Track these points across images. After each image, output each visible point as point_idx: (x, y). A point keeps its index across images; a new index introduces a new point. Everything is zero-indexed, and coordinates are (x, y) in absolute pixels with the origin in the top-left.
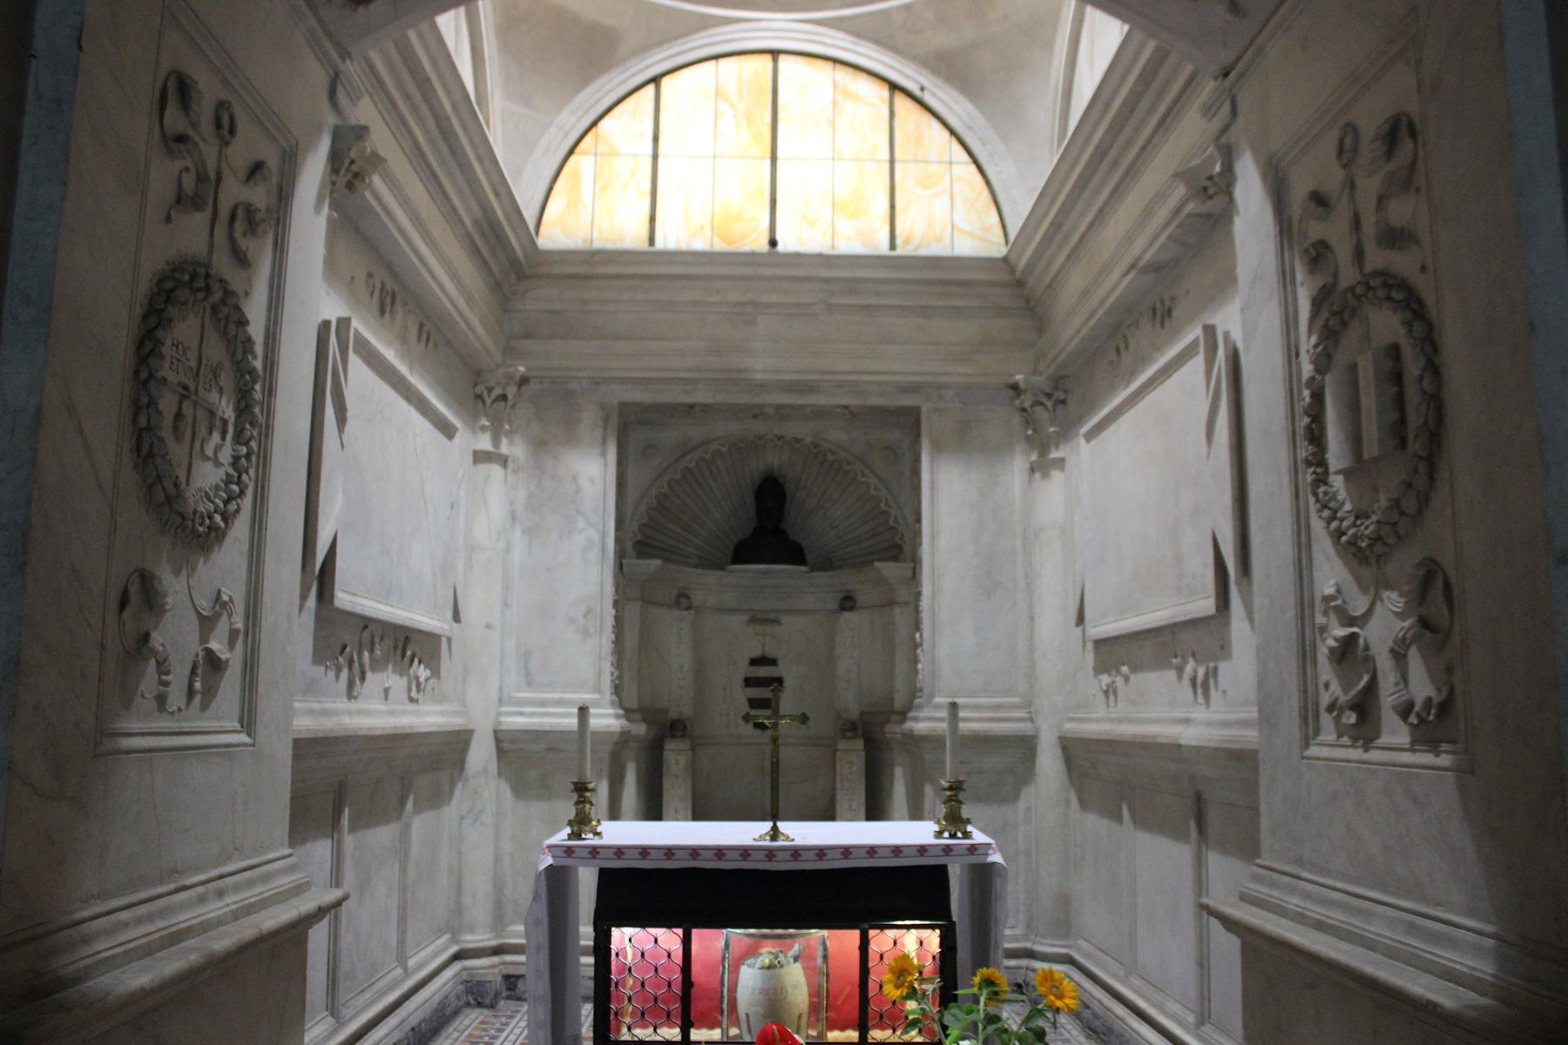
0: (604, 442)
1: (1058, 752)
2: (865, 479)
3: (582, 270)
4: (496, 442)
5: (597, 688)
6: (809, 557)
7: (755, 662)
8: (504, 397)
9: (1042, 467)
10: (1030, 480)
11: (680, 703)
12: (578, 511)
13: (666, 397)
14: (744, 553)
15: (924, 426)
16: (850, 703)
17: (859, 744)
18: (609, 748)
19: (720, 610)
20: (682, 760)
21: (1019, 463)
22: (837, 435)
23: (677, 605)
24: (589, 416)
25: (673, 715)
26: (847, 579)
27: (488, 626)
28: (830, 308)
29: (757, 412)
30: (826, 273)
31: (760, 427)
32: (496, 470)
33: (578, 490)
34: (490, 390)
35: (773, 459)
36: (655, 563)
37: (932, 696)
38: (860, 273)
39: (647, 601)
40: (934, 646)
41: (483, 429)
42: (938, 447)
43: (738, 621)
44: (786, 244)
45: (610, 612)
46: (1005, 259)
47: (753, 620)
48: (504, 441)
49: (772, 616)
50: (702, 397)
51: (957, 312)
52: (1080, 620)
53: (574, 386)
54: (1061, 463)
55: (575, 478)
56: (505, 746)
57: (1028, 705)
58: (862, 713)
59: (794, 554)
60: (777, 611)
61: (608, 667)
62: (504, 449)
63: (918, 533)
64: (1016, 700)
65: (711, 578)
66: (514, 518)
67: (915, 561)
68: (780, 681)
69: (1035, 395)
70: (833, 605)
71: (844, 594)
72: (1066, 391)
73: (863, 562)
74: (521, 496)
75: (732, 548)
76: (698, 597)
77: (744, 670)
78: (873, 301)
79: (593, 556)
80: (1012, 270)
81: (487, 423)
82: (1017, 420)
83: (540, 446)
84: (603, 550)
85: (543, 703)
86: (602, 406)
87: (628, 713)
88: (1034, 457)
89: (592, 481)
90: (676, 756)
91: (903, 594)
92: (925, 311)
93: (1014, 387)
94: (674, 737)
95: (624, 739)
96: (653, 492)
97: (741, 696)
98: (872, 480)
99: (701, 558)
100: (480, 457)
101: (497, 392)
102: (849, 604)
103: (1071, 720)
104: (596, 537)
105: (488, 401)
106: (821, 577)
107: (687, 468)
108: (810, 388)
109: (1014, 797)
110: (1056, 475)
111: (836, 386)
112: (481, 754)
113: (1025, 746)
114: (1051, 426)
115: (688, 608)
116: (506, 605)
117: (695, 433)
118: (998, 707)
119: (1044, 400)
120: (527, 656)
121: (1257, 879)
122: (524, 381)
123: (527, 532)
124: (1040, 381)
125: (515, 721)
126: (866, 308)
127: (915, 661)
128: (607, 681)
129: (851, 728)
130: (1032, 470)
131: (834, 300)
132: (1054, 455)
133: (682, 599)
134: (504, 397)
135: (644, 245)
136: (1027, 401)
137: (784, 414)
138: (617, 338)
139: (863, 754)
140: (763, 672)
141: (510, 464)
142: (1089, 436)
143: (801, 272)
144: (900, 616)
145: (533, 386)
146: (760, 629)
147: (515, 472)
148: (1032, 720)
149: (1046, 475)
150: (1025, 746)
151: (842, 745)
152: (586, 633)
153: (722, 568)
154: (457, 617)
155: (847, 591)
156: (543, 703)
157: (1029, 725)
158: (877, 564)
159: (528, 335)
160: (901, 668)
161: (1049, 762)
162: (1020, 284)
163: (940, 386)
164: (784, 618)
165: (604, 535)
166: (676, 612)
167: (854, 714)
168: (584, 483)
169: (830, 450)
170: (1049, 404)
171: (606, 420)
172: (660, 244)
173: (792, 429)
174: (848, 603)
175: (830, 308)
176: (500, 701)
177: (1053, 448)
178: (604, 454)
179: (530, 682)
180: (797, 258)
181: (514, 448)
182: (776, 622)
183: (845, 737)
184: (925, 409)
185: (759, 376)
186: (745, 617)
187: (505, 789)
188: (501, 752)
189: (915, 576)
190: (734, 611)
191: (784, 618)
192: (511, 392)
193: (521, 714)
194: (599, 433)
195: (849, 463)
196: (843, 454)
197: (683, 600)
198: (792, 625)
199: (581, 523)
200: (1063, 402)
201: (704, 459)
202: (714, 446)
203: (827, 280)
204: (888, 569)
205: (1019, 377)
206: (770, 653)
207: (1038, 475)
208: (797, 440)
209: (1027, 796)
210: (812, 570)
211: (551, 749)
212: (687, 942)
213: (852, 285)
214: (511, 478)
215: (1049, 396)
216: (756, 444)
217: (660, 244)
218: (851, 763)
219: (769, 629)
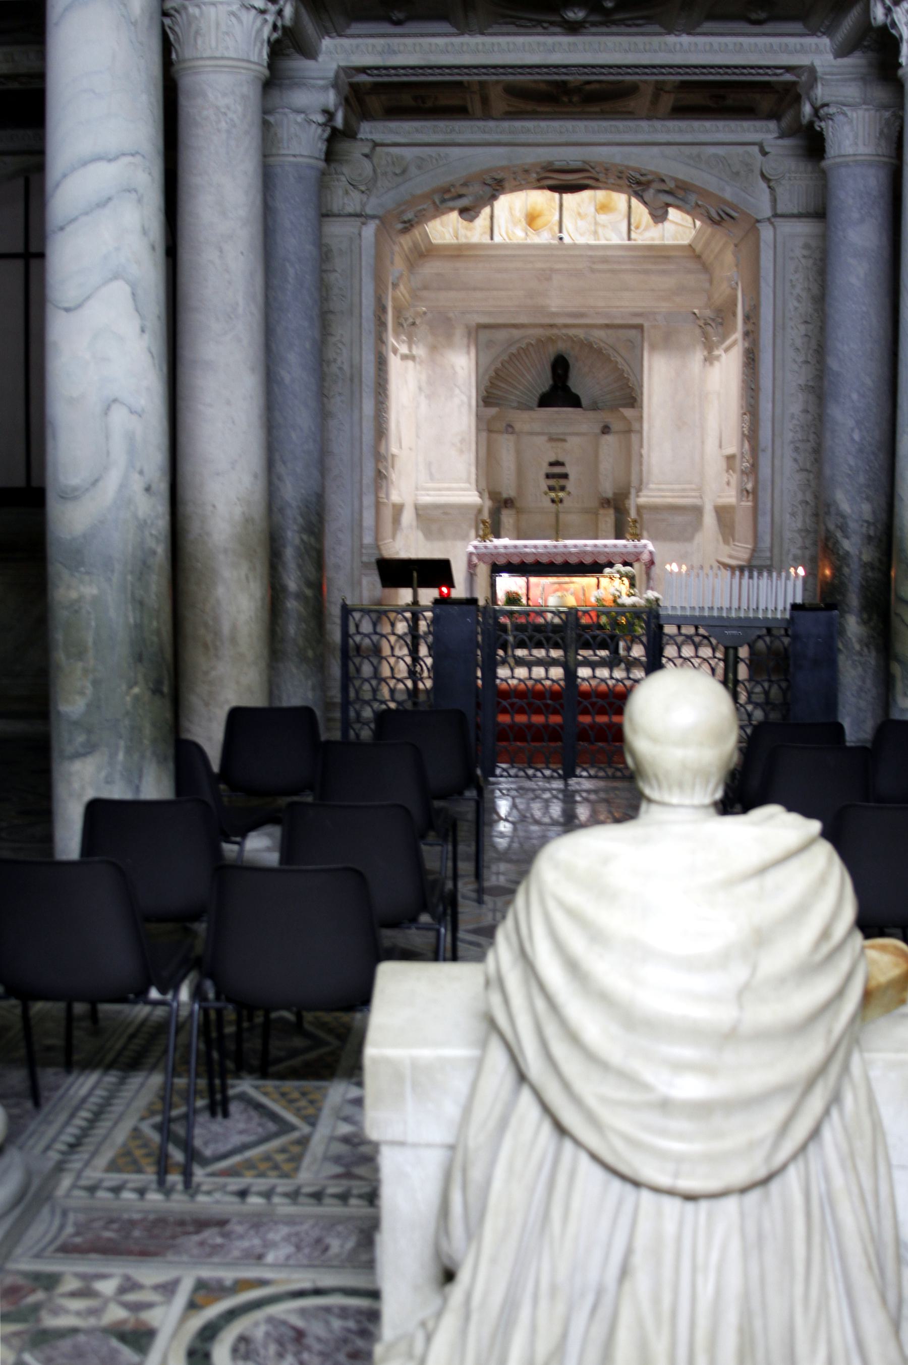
0: (468, 346)
1: (713, 514)
2: (615, 358)
3: (455, 253)
4: (410, 349)
5: (470, 483)
6: (584, 401)
7: (552, 464)
8: (414, 324)
9: (709, 359)
10: (704, 366)
11: (509, 491)
12: (455, 385)
13: (501, 321)
14: (545, 401)
15: (646, 335)
16: (608, 489)
17: (611, 512)
18: (475, 512)
19: (532, 434)
20: (511, 521)
21: (699, 355)
22: (598, 335)
23: (507, 432)
24: (459, 334)
25: (505, 496)
26: (606, 417)
27: (411, 449)
28: (593, 271)
29: (552, 326)
30: (590, 253)
31: (555, 331)
32: (410, 363)
33: (455, 373)
34: (406, 319)
35: (561, 347)
36: (493, 411)
37: (648, 484)
38: (609, 253)
39: (490, 431)
40: (649, 456)
41: (403, 342)
42: (653, 348)
43: (541, 440)
44: (567, 240)
45: (473, 438)
46: (690, 246)
47: (551, 440)
48: (414, 347)
49: (561, 437)
50: (523, 319)
51: (664, 272)
52: (720, 446)
53: (451, 315)
54: (718, 358)
55: (453, 367)
56: (420, 512)
57: (700, 489)
58: (615, 494)
59: (574, 402)
60: (565, 434)
61: (473, 470)
62: (415, 351)
63: (642, 394)
64: (693, 486)
65: (526, 415)
66: (420, 389)
67: (641, 407)
68: (565, 476)
69: (705, 320)
70: (597, 430)
71: (602, 425)
72: (722, 318)
73: (614, 408)
74: (424, 377)
75: (538, 396)
76: (518, 426)
77: (546, 468)
78: (616, 267)
79: (465, 410)
80: (694, 250)
81: (405, 338)
82: (698, 331)
83: (433, 349)
84: (470, 406)
85: (440, 490)
86: (467, 326)
87: (481, 496)
88: (706, 353)
89: (463, 368)
90: (508, 518)
91: (636, 426)
92: (646, 272)
93: (694, 314)
94: (506, 507)
95: (480, 511)
96: (493, 368)
97: (544, 484)
98: (619, 360)
99: (519, 402)
100: (404, 357)
101: (411, 320)
102: (606, 430)
103: (719, 497)
104: (465, 399)
105: (405, 325)
106: (591, 414)
107: (513, 354)
108: (582, 315)
109: (690, 539)
110: (716, 363)
111: (596, 313)
112: (408, 517)
113: (698, 511)
114: (715, 337)
115: (512, 433)
116: (418, 436)
117: (516, 333)
118: (684, 490)
119: (710, 322)
120: (429, 465)
121: (733, 550)
122: (425, 313)
123: (428, 397)
124: (708, 313)
125: (427, 499)
126: (613, 271)
127: (641, 464)
128: (473, 477)
129: (606, 503)
130: (706, 360)
131: (596, 266)
132: (716, 353)
133: (510, 428)
134: (414, 324)
135: (489, 241)
136: (701, 323)
137: (566, 326)
138: (475, 289)
139: (613, 517)
140: (557, 470)
141: (418, 359)
142: (727, 350)
143: (577, 252)
144: (634, 437)
145: (429, 315)
146: (554, 444)
147: (421, 363)
148: (701, 498)
149: (711, 364)
150: (698, 511)
151: (601, 512)
152: (461, 452)
153: (530, 408)
154: (401, 447)
155: (606, 422)
156: (440, 490)
157: (700, 500)
158: (622, 410)
159: (425, 288)
160: (635, 469)
161: (709, 519)
162: (698, 257)
163: (655, 313)
164: (568, 438)
165: (470, 398)
166: (506, 436)
167: (609, 494)
168: (458, 369)
169: (594, 342)
170: (713, 324)
171: (469, 334)
172: (498, 239)
173: (572, 332)
174: (606, 430)
175: (593, 271)
176: (417, 489)
177: (715, 349)
178: (468, 353)
179: (432, 477)
180: (575, 246)
181: (420, 351)
182: (564, 440)
183: (603, 507)
184: (646, 325)
185: (554, 310)
186: (545, 438)
187: (420, 535)
188: (418, 515)
189: (641, 418)
190: (538, 434)
191: (568, 438)
192: (418, 321)
193: (428, 495)
194: (465, 341)
195: (606, 350)
196: (602, 345)
197: (510, 430)
198: (573, 442)
199: (457, 391)
200: (721, 324)
201: (522, 348)
202: (527, 341)
203: (591, 257)
204: (628, 412)
205: (696, 311)
206: (561, 459)
207: (707, 364)
208: (576, 336)
209: (699, 538)
210: (585, 410)
211: (445, 513)
212: (528, 583)
213: (605, 260)
214: (418, 367)
215: (713, 320)
216: (551, 340)
217: (498, 239)
218: (606, 521)
219: (560, 444)
